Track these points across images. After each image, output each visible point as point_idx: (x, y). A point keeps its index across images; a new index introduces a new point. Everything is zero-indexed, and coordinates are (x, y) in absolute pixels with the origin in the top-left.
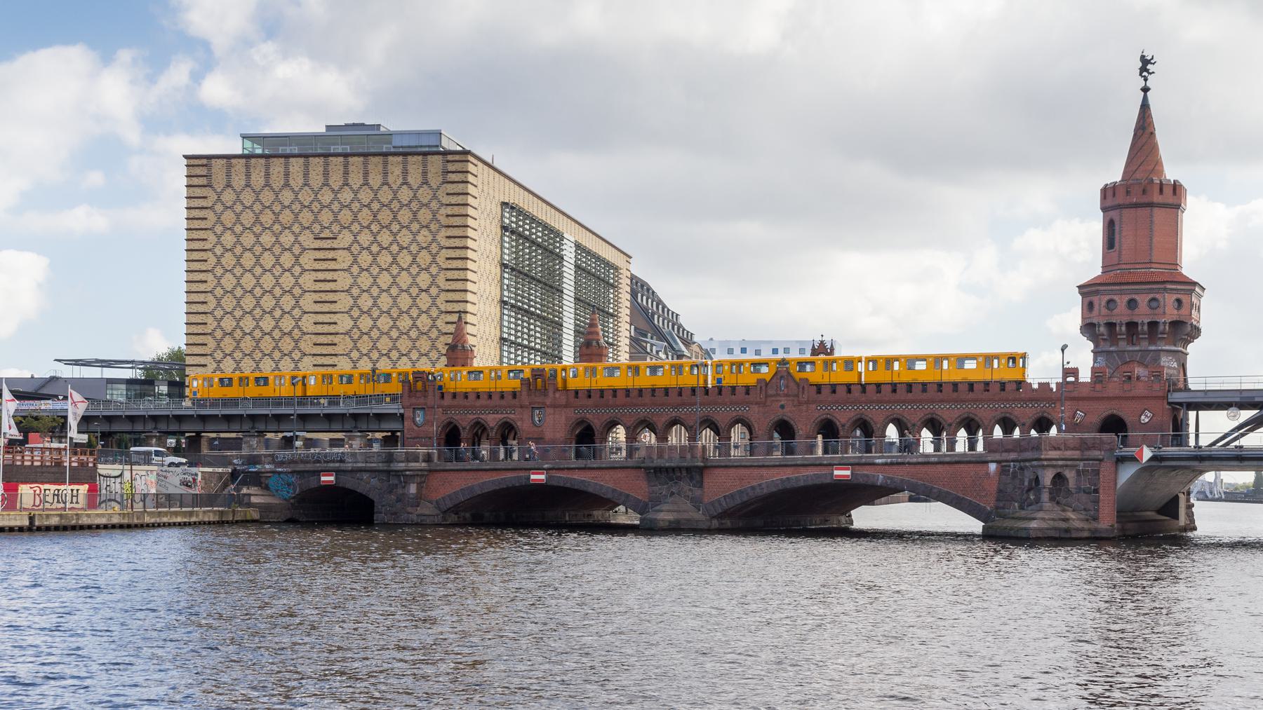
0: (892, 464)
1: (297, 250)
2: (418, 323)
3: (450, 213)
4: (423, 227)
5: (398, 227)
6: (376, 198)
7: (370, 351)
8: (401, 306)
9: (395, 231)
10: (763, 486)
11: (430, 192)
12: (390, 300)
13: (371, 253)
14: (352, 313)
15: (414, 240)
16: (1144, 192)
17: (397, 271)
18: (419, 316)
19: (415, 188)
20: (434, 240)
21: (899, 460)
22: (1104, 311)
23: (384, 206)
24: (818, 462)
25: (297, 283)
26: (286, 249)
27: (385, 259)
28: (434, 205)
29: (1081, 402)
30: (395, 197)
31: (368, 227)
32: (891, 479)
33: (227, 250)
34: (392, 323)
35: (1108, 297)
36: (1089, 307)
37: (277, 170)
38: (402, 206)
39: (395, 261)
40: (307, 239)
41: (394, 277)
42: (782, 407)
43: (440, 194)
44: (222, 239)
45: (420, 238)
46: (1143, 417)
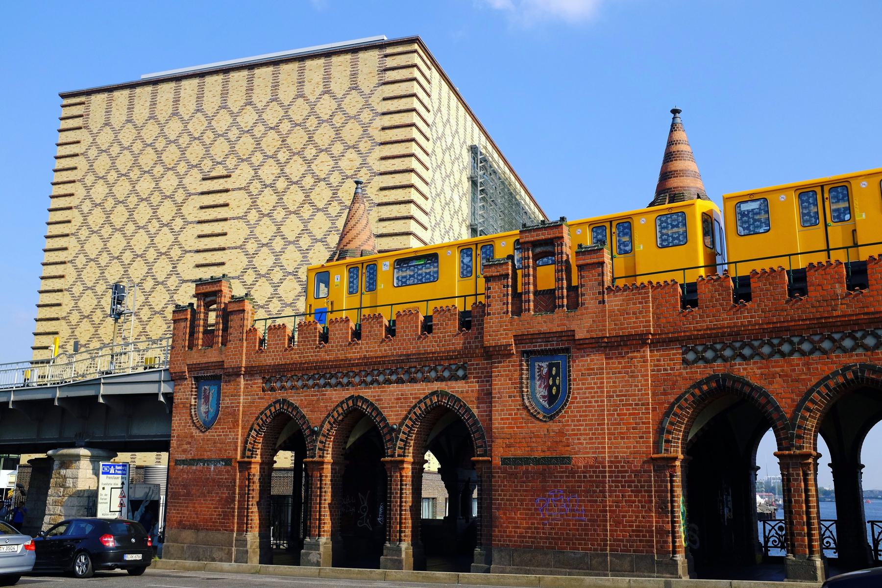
1: (180, 196)
3: (387, 124)
4: (349, 147)
5: (314, 151)
9: (309, 157)
11: (360, 99)
12: (298, 256)
14: (246, 278)
15: (336, 168)
17: (310, 213)
19: (340, 96)
20: (364, 164)
23: (297, 125)
25: (176, 241)
26: (167, 197)
27: (294, 197)
30: (312, 112)
33: (96, 205)
37: (165, 98)
40: (194, 182)
41: (305, 222)
44: (91, 191)
45: (344, 164)
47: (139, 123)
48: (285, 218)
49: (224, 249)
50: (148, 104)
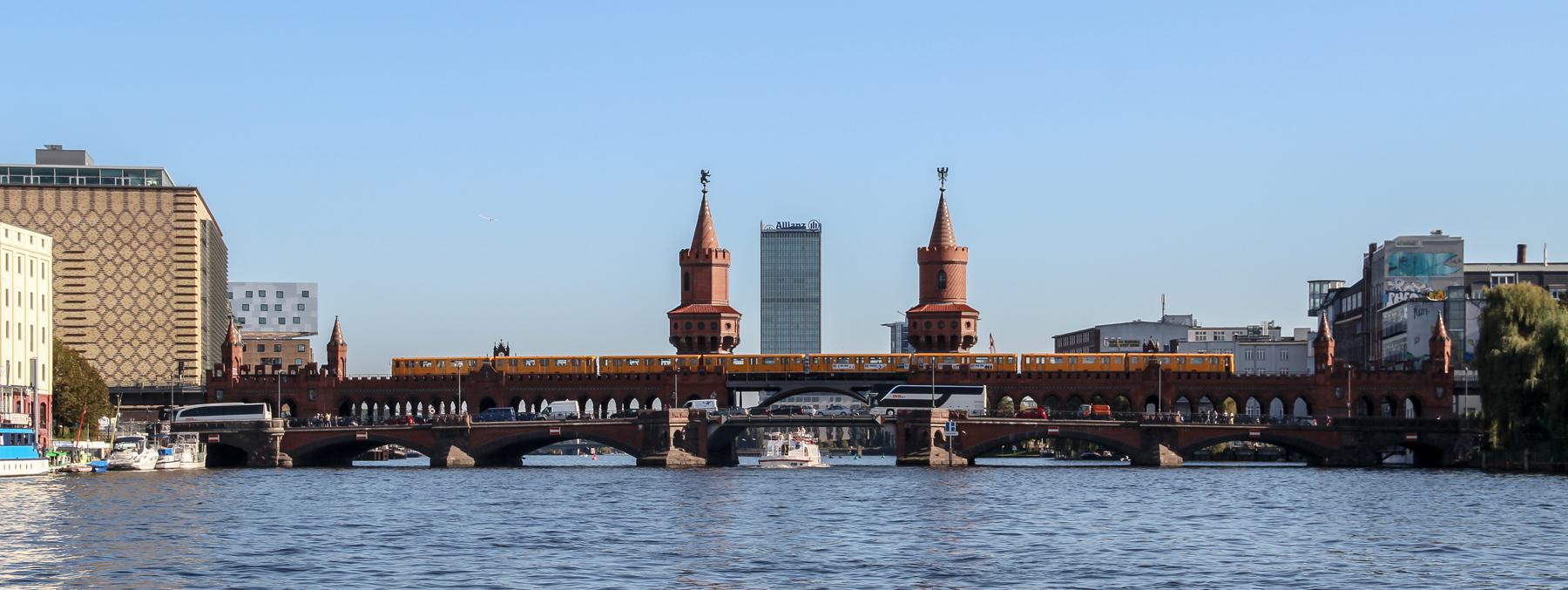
2: (155, 318)
3: (180, 235)
6: (118, 221)
7: (115, 340)
8: (141, 305)
12: (132, 301)
13: (114, 264)
15: (151, 255)
18: (156, 313)
20: (167, 255)
27: (126, 269)
28: (167, 228)
31: (112, 244)
34: (133, 318)
35: (686, 321)
36: (674, 326)
38: (140, 228)
39: (135, 270)
42: (487, 389)
43: (172, 219)
45: (156, 253)
47: (15, 211)
48: (122, 279)
49: (84, 293)
50: (20, 199)
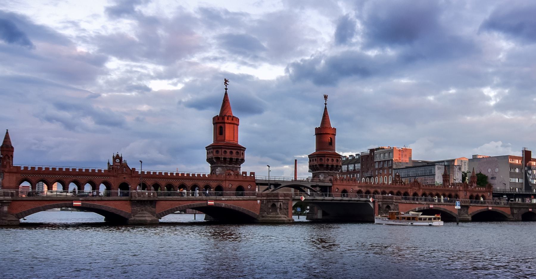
0: (228, 200)
10: (181, 207)
16: (232, 120)
21: (230, 199)
22: (223, 153)
24: (202, 199)
29: (231, 182)
32: (226, 205)
46: (248, 187)
